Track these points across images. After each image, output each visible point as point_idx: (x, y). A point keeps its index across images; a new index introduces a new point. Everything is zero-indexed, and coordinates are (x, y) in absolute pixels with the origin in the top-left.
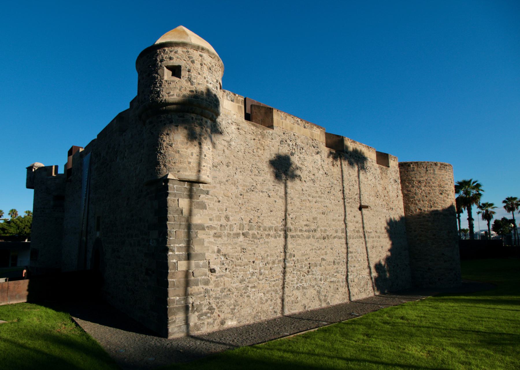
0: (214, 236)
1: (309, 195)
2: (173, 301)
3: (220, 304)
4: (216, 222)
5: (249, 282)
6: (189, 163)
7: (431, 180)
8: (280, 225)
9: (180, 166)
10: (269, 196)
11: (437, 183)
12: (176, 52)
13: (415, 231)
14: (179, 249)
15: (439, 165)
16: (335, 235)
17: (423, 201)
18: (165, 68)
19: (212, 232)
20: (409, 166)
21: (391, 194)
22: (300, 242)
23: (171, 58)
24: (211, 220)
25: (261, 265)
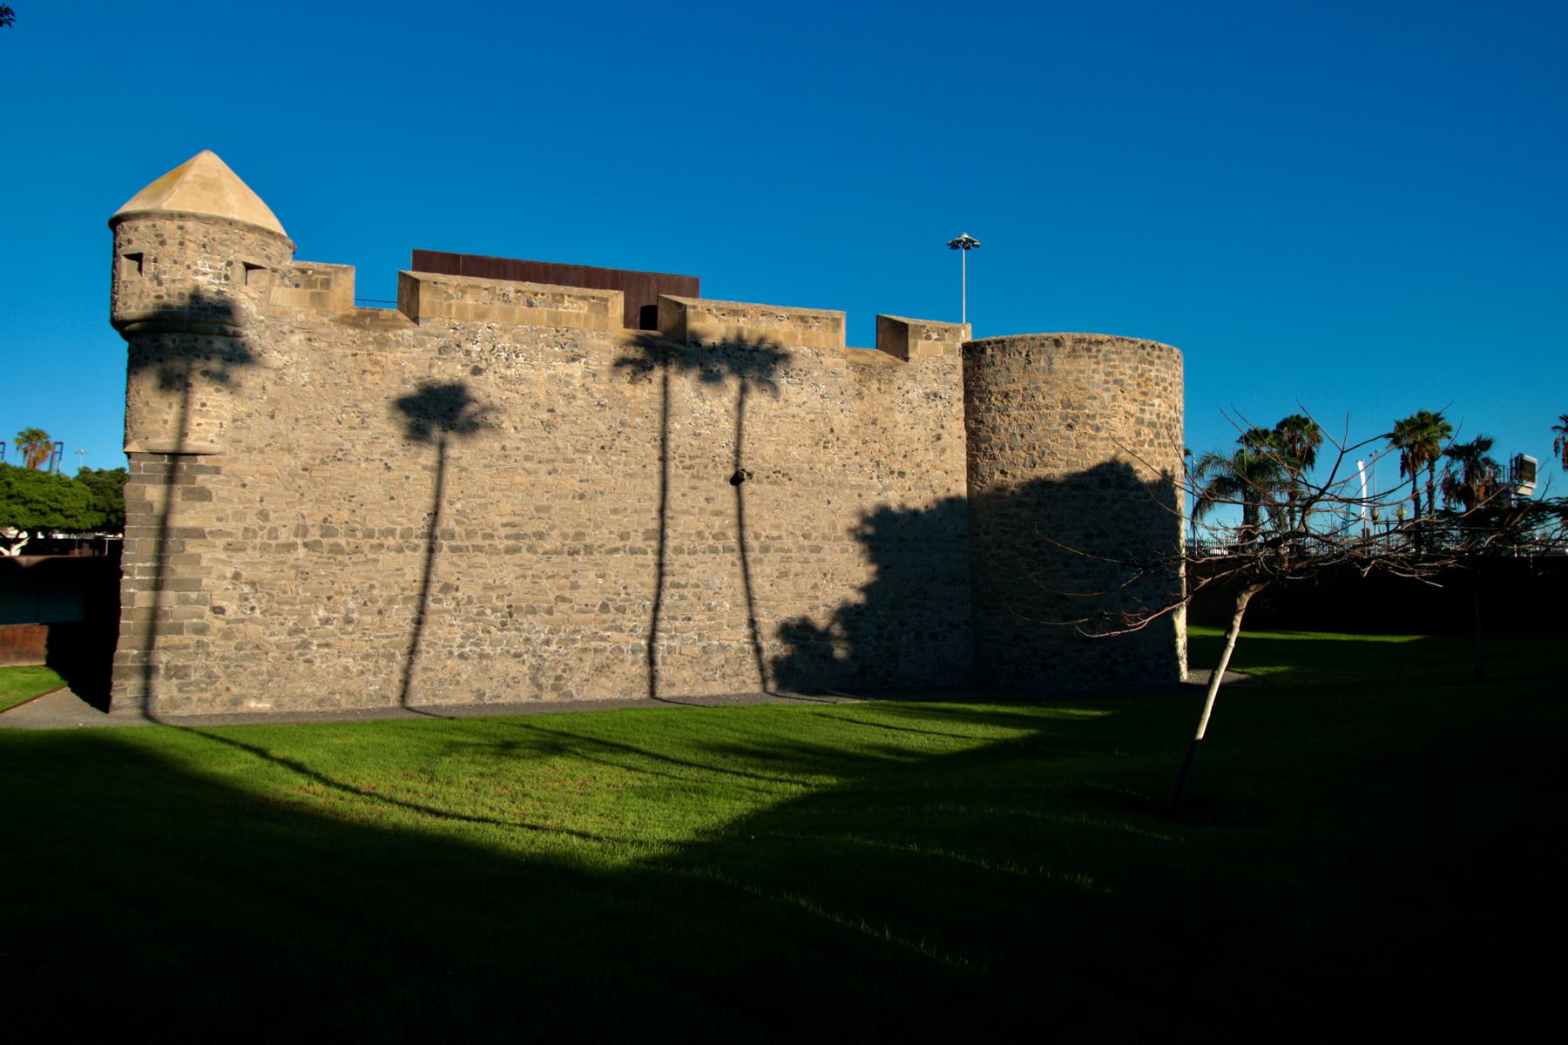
0: (225, 549)
1: (527, 458)
2: (126, 656)
3: (232, 669)
4: (234, 524)
5: (312, 636)
6: (166, 422)
7: (1037, 388)
8: (419, 524)
9: (150, 428)
10: (389, 468)
11: (1059, 396)
12: (136, 230)
13: (987, 533)
14: (142, 571)
15: (1069, 344)
16: (620, 544)
17: (1012, 449)
18: (124, 260)
19: (221, 542)
20: (983, 351)
21: (901, 432)
22: (484, 560)
23: (130, 242)
24: (220, 519)
25: (351, 605)
